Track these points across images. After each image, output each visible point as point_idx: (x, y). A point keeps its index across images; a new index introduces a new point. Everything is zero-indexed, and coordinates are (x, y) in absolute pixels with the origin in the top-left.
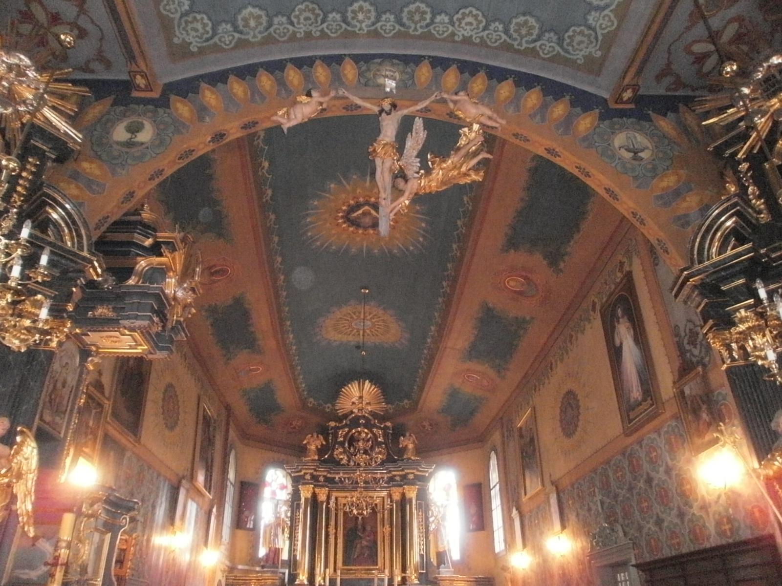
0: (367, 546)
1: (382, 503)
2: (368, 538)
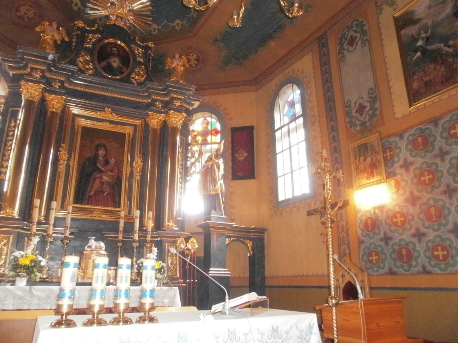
0: (107, 182)
1: (132, 133)
2: (110, 173)
